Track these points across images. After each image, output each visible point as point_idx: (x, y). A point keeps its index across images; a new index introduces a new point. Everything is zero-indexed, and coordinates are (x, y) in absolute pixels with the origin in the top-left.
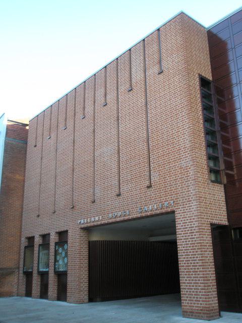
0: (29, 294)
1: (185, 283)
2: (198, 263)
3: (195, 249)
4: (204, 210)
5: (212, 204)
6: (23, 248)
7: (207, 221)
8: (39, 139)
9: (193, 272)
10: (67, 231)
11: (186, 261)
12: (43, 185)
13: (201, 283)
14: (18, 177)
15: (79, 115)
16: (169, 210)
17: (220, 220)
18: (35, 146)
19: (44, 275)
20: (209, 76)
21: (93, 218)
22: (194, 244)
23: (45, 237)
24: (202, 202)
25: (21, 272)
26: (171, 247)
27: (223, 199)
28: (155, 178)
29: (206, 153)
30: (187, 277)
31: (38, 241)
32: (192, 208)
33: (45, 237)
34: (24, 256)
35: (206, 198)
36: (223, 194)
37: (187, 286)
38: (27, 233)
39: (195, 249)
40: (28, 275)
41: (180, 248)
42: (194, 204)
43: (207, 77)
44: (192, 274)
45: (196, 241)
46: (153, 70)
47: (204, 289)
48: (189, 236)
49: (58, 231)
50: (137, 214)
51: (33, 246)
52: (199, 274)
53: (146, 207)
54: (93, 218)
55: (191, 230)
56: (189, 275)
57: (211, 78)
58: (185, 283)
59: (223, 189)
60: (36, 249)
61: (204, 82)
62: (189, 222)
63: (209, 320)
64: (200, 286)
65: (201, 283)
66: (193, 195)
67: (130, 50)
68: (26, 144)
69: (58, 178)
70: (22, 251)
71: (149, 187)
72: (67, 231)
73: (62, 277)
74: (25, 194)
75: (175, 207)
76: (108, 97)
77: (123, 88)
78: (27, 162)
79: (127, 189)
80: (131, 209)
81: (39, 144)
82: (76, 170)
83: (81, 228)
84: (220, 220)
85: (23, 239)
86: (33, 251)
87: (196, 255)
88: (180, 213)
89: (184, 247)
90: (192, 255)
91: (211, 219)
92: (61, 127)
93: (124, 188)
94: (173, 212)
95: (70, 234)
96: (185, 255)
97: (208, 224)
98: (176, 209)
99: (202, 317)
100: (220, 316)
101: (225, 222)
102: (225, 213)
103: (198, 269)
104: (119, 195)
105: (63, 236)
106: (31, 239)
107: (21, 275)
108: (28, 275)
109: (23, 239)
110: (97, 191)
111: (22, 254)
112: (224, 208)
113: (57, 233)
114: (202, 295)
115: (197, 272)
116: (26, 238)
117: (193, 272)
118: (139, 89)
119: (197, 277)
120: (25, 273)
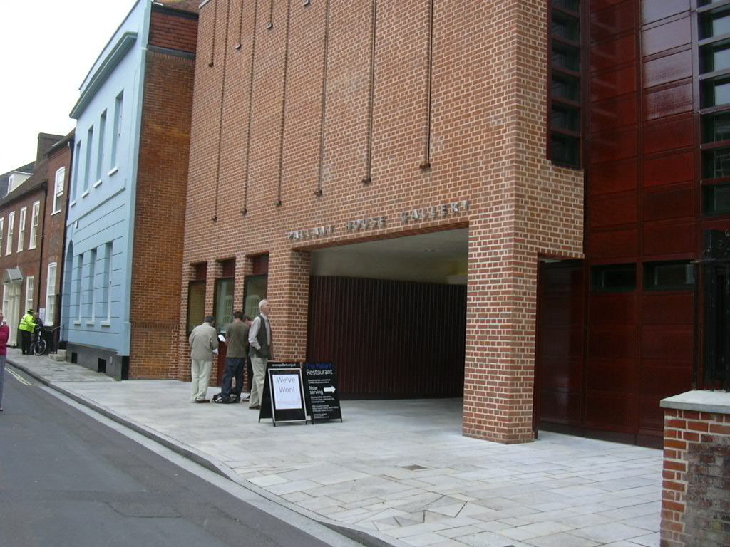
1: (473, 371)
2: (500, 332)
3: (498, 304)
4: (526, 224)
5: (547, 211)
6: (185, 284)
7: (532, 248)
8: (220, 48)
9: (490, 349)
10: (266, 255)
11: (479, 327)
12: (224, 153)
13: (501, 373)
14: (175, 132)
16: (459, 219)
17: (564, 248)
18: (211, 65)
21: (316, 229)
22: (498, 293)
23: (227, 264)
24: (523, 207)
26: (459, 295)
28: (437, 149)
29: (548, 98)
30: (478, 360)
31: (212, 270)
34: (189, 302)
35: (536, 199)
36: (580, 190)
37: (475, 376)
38: (192, 254)
39: (498, 304)
41: (471, 299)
42: (508, 208)
44: (488, 355)
45: (500, 287)
47: (505, 385)
48: (489, 276)
49: (250, 252)
50: (398, 225)
51: (205, 282)
52: (499, 355)
53: (415, 211)
54: (316, 229)
55: (495, 265)
56: (482, 355)
58: (473, 371)
59: (580, 180)
60: (210, 287)
62: (493, 248)
63: (507, 443)
64: (498, 378)
65: (501, 373)
66: (506, 191)
68: (194, 58)
70: (185, 290)
71: (426, 167)
72: (266, 255)
75: (470, 213)
78: (195, 100)
79: (382, 168)
80: (389, 212)
81: (218, 62)
82: (289, 123)
83: (294, 250)
84: (564, 248)
85: (186, 266)
87: (497, 316)
88: (477, 228)
89: (478, 299)
90: (491, 316)
91: (540, 244)
92: (263, 23)
93: (378, 168)
94: (465, 225)
95: (272, 260)
96: (479, 316)
97: (533, 254)
98: (472, 218)
99: (496, 436)
100: (536, 437)
101: (575, 250)
102: (579, 233)
103: (499, 344)
104: (367, 181)
105: (259, 261)
106: (200, 267)
109: (186, 266)
110: (326, 171)
111: (185, 296)
112: (580, 222)
113: (248, 256)
114: (500, 396)
115: (496, 350)
116: (191, 265)
117: (490, 349)
119: (496, 361)
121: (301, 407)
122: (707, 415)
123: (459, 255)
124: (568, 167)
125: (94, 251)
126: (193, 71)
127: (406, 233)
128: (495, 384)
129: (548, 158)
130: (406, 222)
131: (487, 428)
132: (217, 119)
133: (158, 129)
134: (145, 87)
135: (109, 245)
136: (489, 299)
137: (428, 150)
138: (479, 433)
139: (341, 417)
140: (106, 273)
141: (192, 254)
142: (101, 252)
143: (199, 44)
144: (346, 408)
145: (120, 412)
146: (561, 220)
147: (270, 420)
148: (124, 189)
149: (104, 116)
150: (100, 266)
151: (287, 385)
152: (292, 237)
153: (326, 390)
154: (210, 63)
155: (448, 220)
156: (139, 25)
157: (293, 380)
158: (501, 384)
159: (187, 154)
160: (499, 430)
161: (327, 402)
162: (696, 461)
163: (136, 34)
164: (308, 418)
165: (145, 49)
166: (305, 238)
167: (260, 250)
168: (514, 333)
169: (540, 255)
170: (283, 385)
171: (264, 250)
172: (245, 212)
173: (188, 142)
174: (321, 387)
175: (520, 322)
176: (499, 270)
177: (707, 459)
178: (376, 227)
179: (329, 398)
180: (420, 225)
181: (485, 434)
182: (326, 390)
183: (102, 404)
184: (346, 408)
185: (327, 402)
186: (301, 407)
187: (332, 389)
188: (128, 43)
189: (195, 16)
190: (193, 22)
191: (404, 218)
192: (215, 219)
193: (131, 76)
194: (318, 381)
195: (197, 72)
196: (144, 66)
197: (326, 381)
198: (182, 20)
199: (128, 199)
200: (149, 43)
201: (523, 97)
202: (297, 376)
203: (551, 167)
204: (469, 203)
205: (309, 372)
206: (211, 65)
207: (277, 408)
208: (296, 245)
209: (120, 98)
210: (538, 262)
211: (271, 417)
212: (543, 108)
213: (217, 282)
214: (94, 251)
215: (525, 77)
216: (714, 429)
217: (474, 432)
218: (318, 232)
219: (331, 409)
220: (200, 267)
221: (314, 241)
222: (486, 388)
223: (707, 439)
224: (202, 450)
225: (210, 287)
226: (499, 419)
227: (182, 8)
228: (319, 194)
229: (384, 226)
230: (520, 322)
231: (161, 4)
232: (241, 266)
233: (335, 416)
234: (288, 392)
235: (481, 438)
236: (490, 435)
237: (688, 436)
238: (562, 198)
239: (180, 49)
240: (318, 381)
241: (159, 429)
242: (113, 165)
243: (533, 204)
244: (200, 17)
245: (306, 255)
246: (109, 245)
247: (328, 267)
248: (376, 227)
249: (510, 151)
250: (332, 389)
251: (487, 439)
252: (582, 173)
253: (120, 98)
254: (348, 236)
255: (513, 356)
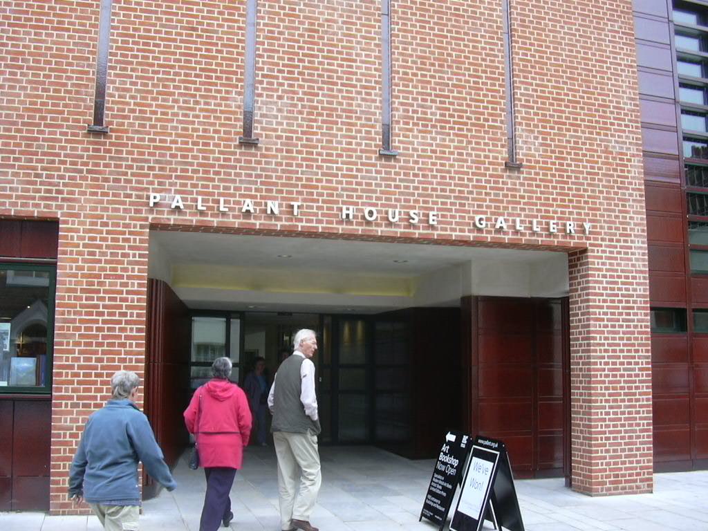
2: (637, 375)
3: (633, 345)
13: (641, 419)
22: (633, 333)
32: (632, 254)
39: (633, 345)
45: (636, 327)
48: (621, 314)
52: (637, 400)
64: (638, 425)
65: (641, 419)
87: (634, 357)
90: (624, 357)
98: (591, 245)
99: (638, 487)
103: (637, 388)
114: (641, 443)
115: (634, 394)
117: (626, 394)
119: (634, 406)
121: (477, 519)
128: (635, 431)
136: (621, 339)
138: (616, 489)
158: (642, 431)
176: (632, 308)
181: (624, 488)
186: (477, 519)
217: (609, 489)
222: (623, 438)
226: (641, 468)
235: (620, 494)
236: (631, 488)
251: (626, 493)
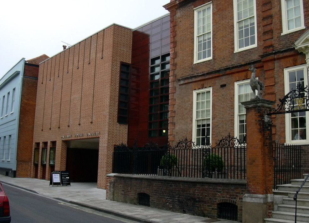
0: (36, 177)
6: (33, 149)
8: (45, 78)
12: (45, 111)
14: (31, 102)
15: (66, 70)
16: (98, 136)
19: (44, 166)
20: (129, 61)
23: (45, 144)
25: (32, 163)
27: (127, 132)
28: (94, 119)
33: (45, 144)
35: (114, 132)
38: (36, 140)
40: (36, 166)
43: (127, 62)
46: (99, 55)
49: (51, 141)
51: (39, 149)
54: (68, 136)
57: (130, 63)
59: (127, 127)
60: (41, 150)
61: (123, 65)
67: (91, 37)
68: (37, 79)
69: (53, 108)
70: (33, 151)
71: (92, 123)
72: (56, 141)
73: (52, 167)
74: (36, 114)
76: (80, 63)
77: (87, 60)
81: (44, 83)
82: (62, 105)
83: (62, 141)
85: (34, 143)
86: (39, 151)
91: (115, 143)
94: (99, 137)
95: (57, 143)
104: (80, 124)
105: (54, 143)
106: (38, 144)
107: (32, 165)
108: (36, 166)
109: (34, 143)
111: (33, 152)
112: (126, 137)
113: (51, 142)
116: (35, 143)
118: (93, 63)
120: (34, 164)
122: (111, 177)
123: (98, 144)
124: (123, 124)
125: (5, 137)
126: (37, 83)
127: (87, 139)
129: (117, 122)
130: (87, 136)
131: (102, 186)
132: (43, 100)
133: (26, 101)
134: (22, 89)
135: (10, 136)
137: (92, 119)
139: (70, 185)
140: (9, 144)
141: (36, 140)
142: (7, 138)
143: (39, 76)
144: (71, 184)
145: (15, 184)
146: (121, 137)
147: (52, 185)
148: (15, 119)
149: (9, 93)
150: (7, 142)
151: (57, 176)
152: (62, 137)
153: (67, 178)
154: (42, 82)
155: (96, 136)
156: (21, 68)
157: (58, 175)
159: (35, 109)
160: (104, 187)
161: (66, 181)
162: (110, 184)
163: (20, 72)
164: (62, 185)
165: (22, 77)
166: (65, 138)
167: (54, 140)
168: (107, 164)
169: (114, 145)
170: (55, 176)
171: (55, 140)
172: (50, 129)
173: (35, 105)
174: (65, 177)
175: (109, 161)
177: (111, 184)
178: (81, 137)
179: (67, 180)
180: (90, 137)
182: (67, 178)
183: (9, 182)
184: (71, 184)
185: (66, 181)
187: (68, 178)
188: (17, 74)
189: (38, 66)
190: (37, 68)
191: (87, 135)
192: (42, 130)
193: (18, 83)
194: (65, 176)
195: (38, 84)
196: (22, 82)
197: (66, 176)
198: (34, 67)
199: (16, 123)
200: (24, 75)
201: (111, 108)
202: (59, 174)
203: (118, 125)
204: (99, 133)
205: (62, 173)
206: (42, 83)
207: (54, 182)
208: (63, 139)
209: (14, 89)
210: (114, 147)
211: (52, 184)
212: (117, 111)
213: (43, 149)
214: (5, 137)
215: (112, 103)
216: (112, 179)
218: (68, 137)
219: (68, 182)
220: (38, 144)
221: (67, 139)
223: (111, 181)
224: (34, 190)
225: (41, 150)
227: (34, 63)
228: (69, 126)
229: (83, 136)
230: (109, 161)
231: (27, 63)
232: (49, 144)
233: (69, 184)
234: (57, 178)
237: (109, 180)
238: (121, 132)
239: (34, 76)
240: (65, 176)
241: (24, 187)
242: (12, 111)
243: (113, 133)
244: (40, 67)
245: (66, 143)
246: (10, 136)
247: (72, 146)
248: (81, 137)
249: (108, 121)
250: (68, 178)
252: (127, 125)
253: (14, 89)
254: (75, 138)
255: (107, 169)
